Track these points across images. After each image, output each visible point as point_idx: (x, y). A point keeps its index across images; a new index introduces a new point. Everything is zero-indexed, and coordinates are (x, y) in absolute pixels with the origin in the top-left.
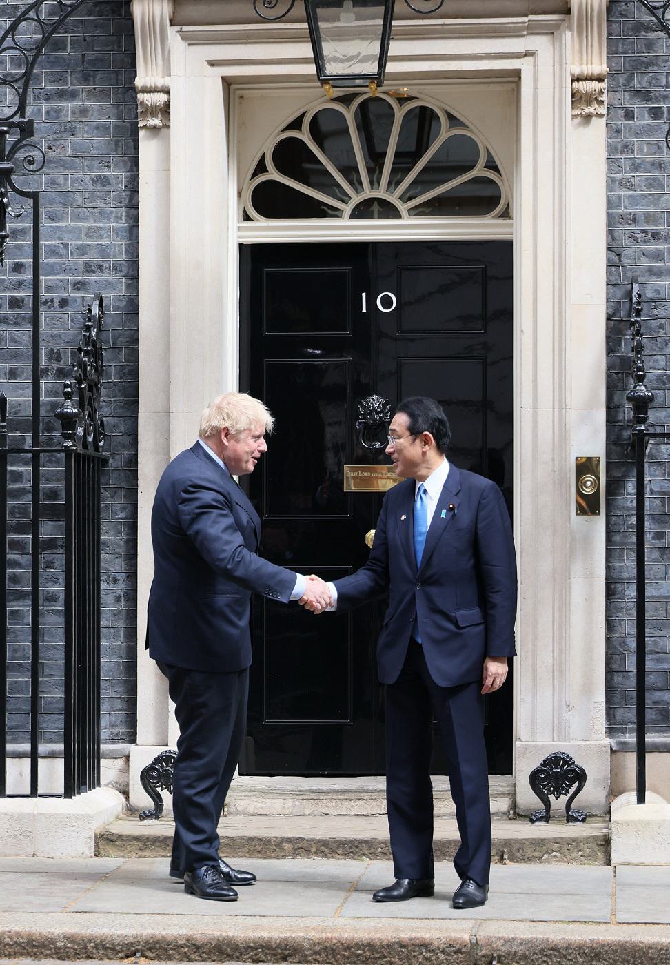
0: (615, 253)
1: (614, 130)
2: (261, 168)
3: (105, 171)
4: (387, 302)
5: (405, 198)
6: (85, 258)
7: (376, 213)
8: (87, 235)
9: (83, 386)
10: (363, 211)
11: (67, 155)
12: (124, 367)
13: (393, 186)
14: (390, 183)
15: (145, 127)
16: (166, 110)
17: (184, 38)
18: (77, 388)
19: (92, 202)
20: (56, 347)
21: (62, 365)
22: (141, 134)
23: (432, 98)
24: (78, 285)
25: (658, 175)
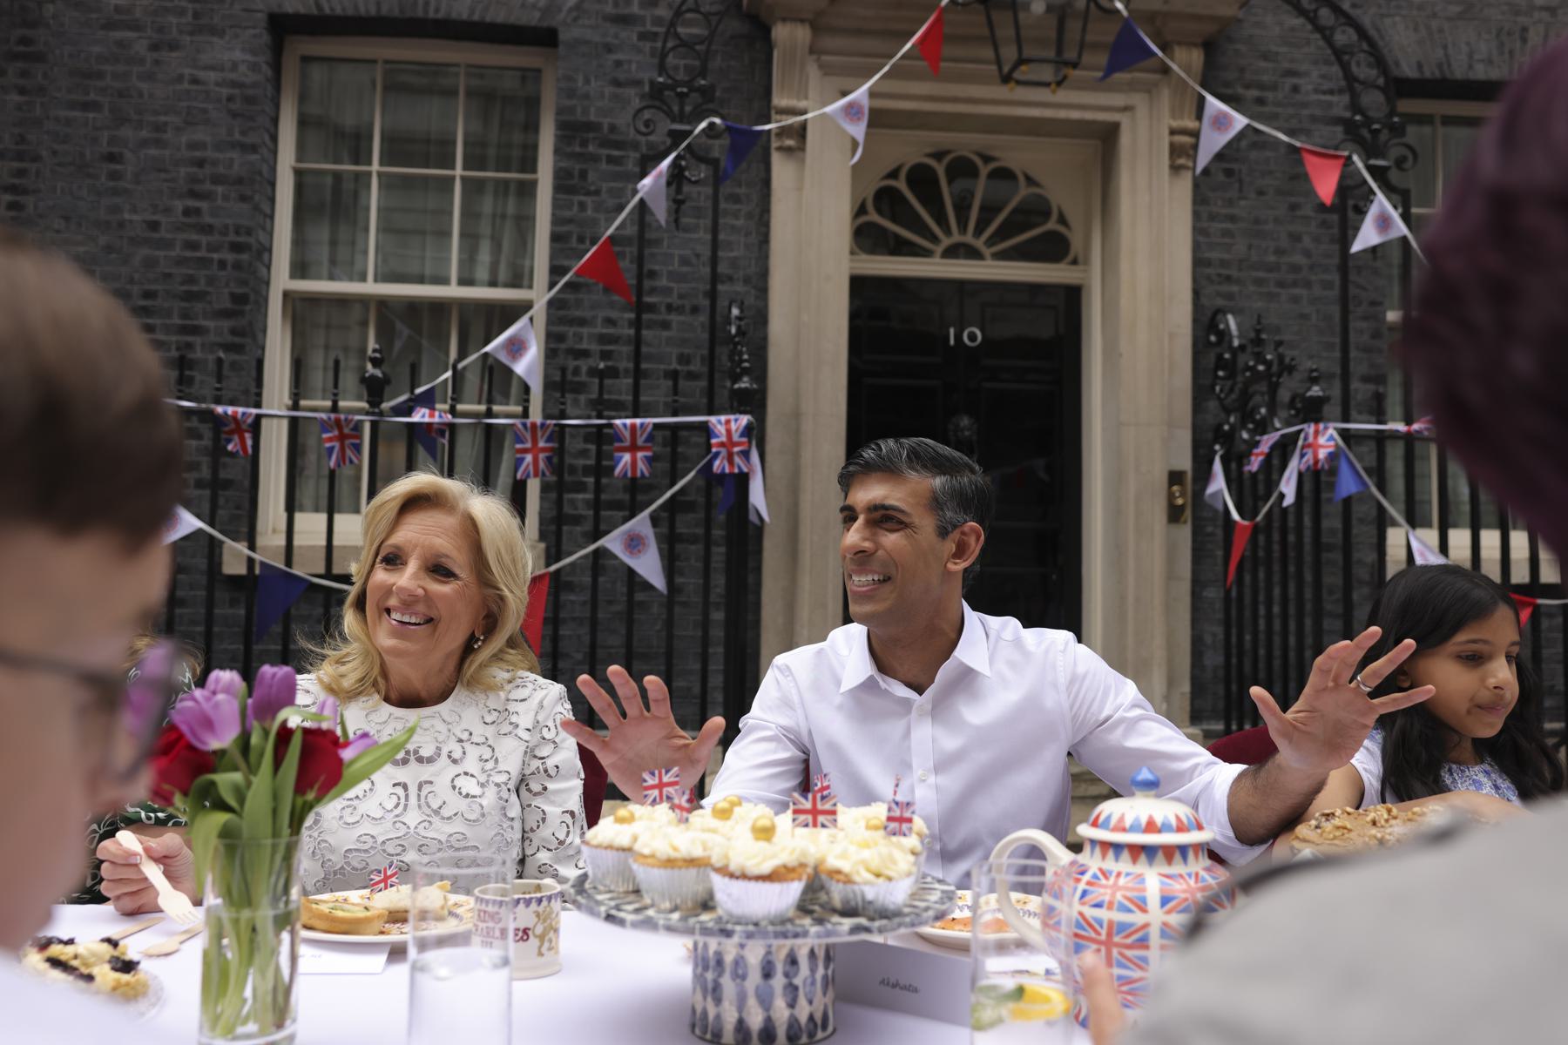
0: (1196, 293)
3: (738, 190)
4: (972, 337)
5: (990, 242)
10: (952, 252)
16: (801, 132)
17: (821, 67)
20: (686, 351)
21: (692, 368)
22: (776, 158)
23: (1018, 154)
25: (1229, 226)
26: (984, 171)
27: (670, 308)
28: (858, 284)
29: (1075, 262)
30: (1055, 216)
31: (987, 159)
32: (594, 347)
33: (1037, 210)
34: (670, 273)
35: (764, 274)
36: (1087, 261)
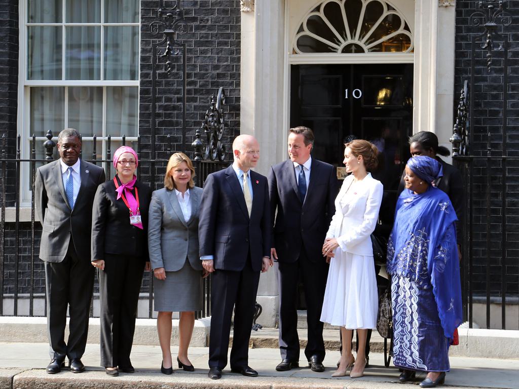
1: (458, 13)
2: (301, 29)
4: (357, 94)
6: (218, 71)
8: (218, 61)
10: (347, 50)
11: (209, 23)
15: (243, 11)
19: (220, 46)
22: (242, 14)
24: (213, 83)
27: (196, 91)
28: (295, 69)
30: (403, 25)
32: (161, 112)
33: (395, 22)
34: (195, 74)
35: (239, 74)
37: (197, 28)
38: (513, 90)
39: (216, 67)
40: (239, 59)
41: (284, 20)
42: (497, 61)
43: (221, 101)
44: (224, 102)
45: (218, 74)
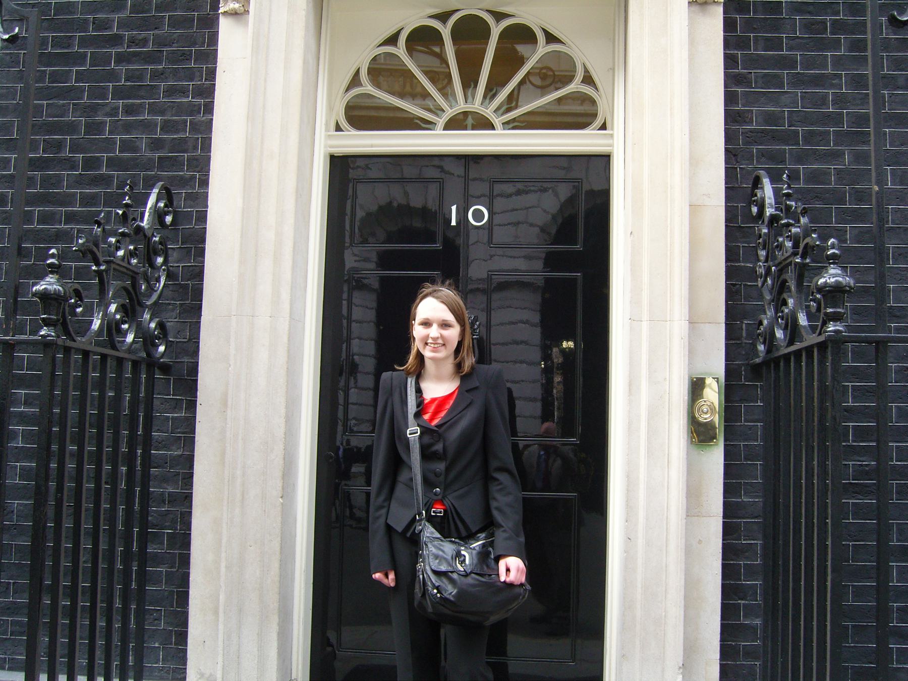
0: (731, 154)
1: (729, 25)
2: (355, 81)
4: (478, 215)
7: (469, 126)
8: (161, 129)
9: (103, 268)
10: (455, 124)
11: (150, 48)
12: (191, 269)
13: (487, 101)
14: (485, 97)
15: (225, 13)
18: (94, 271)
26: (496, 30)
29: (603, 127)
31: (499, 16)
36: (612, 129)
37: (121, 59)
38: (860, 200)
39: (156, 145)
40: (208, 126)
41: (320, 40)
42: (821, 133)
43: (159, 215)
44: (169, 219)
45: (159, 158)
